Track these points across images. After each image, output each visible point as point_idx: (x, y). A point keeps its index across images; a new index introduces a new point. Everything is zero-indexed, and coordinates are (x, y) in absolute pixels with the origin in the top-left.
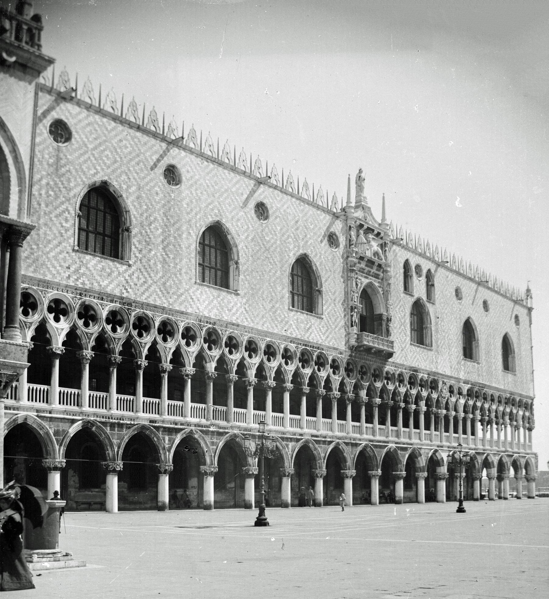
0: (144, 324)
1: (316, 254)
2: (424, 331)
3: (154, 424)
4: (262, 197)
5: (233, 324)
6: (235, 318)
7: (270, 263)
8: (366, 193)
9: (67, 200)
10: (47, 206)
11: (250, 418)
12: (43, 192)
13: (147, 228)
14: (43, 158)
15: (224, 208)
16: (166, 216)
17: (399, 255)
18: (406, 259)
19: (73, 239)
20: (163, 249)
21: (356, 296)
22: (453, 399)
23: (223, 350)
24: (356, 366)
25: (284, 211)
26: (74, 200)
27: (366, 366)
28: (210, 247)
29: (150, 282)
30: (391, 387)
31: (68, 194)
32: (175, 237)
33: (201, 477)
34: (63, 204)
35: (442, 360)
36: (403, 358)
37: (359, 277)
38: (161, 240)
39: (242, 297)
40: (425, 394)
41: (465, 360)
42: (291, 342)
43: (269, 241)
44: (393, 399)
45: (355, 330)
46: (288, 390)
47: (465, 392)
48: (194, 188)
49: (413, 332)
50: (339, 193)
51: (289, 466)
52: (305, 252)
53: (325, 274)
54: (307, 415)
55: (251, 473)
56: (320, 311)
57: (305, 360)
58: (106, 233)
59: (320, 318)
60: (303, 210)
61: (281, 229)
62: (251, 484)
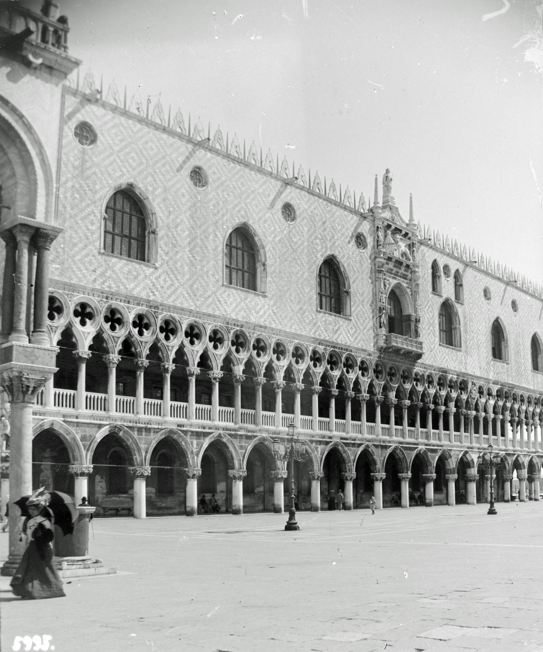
0: (171, 327)
1: (344, 256)
2: (453, 332)
3: (182, 429)
4: (289, 198)
5: (261, 327)
6: (262, 320)
7: (298, 264)
8: (393, 193)
9: (93, 203)
10: (72, 209)
12: (68, 195)
13: (174, 230)
14: (68, 160)
15: (251, 209)
16: (193, 218)
17: (427, 255)
18: (434, 259)
19: (99, 242)
20: (190, 251)
21: (385, 298)
22: (483, 400)
23: (251, 353)
24: (385, 368)
25: (312, 212)
26: (100, 202)
27: (395, 367)
28: (237, 249)
29: (177, 284)
30: (420, 388)
31: (94, 196)
32: (202, 239)
33: (229, 481)
34: (89, 207)
35: (471, 360)
36: (432, 359)
37: (387, 278)
38: (188, 242)
39: (269, 299)
40: (454, 395)
41: (494, 360)
42: (319, 344)
43: (296, 243)
44: (423, 400)
45: (384, 331)
46: (317, 393)
47: (494, 393)
48: (220, 190)
49: (442, 333)
50: (366, 194)
51: (318, 469)
52: (333, 253)
53: (353, 275)
54: (336, 418)
55: (280, 476)
56: (348, 313)
57: (333, 362)
58: (132, 236)
59: (348, 319)
60: (330, 211)
61: (308, 230)
62: (280, 488)
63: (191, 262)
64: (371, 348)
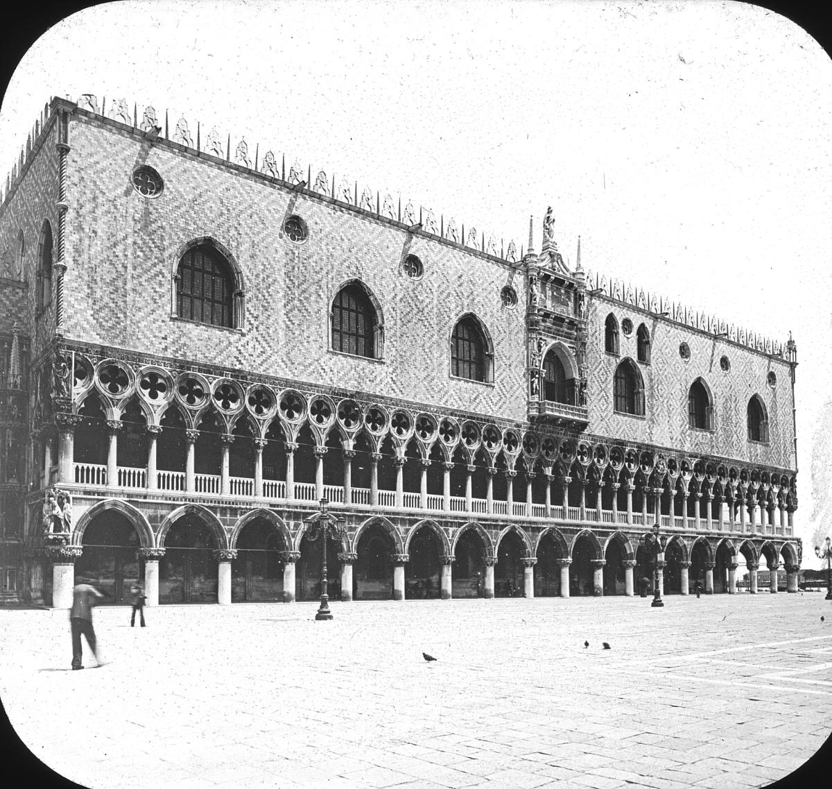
2: (635, 397)
3: (275, 509)
5: (377, 396)
6: (378, 389)
7: (425, 326)
9: (161, 262)
10: (135, 268)
11: (398, 500)
12: (129, 253)
13: (265, 291)
15: (363, 265)
18: (609, 313)
22: (676, 475)
23: (364, 426)
24: (539, 440)
26: (169, 261)
27: (553, 439)
28: (349, 310)
29: (269, 352)
30: (586, 462)
34: (155, 266)
36: (603, 429)
37: (544, 338)
38: (283, 304)
39: (388, 366)
40: (634, 469)
42: (452, 414)
46: (448, 469)
47: (692, 467)
48: (324, 243)
52: (471, 311)
55: (399, 560)
56: (491, 379)
57: (470, 434)
59: (491, 386)
60: (469, 262)
63: (288, 327)
64: (523, 419)
